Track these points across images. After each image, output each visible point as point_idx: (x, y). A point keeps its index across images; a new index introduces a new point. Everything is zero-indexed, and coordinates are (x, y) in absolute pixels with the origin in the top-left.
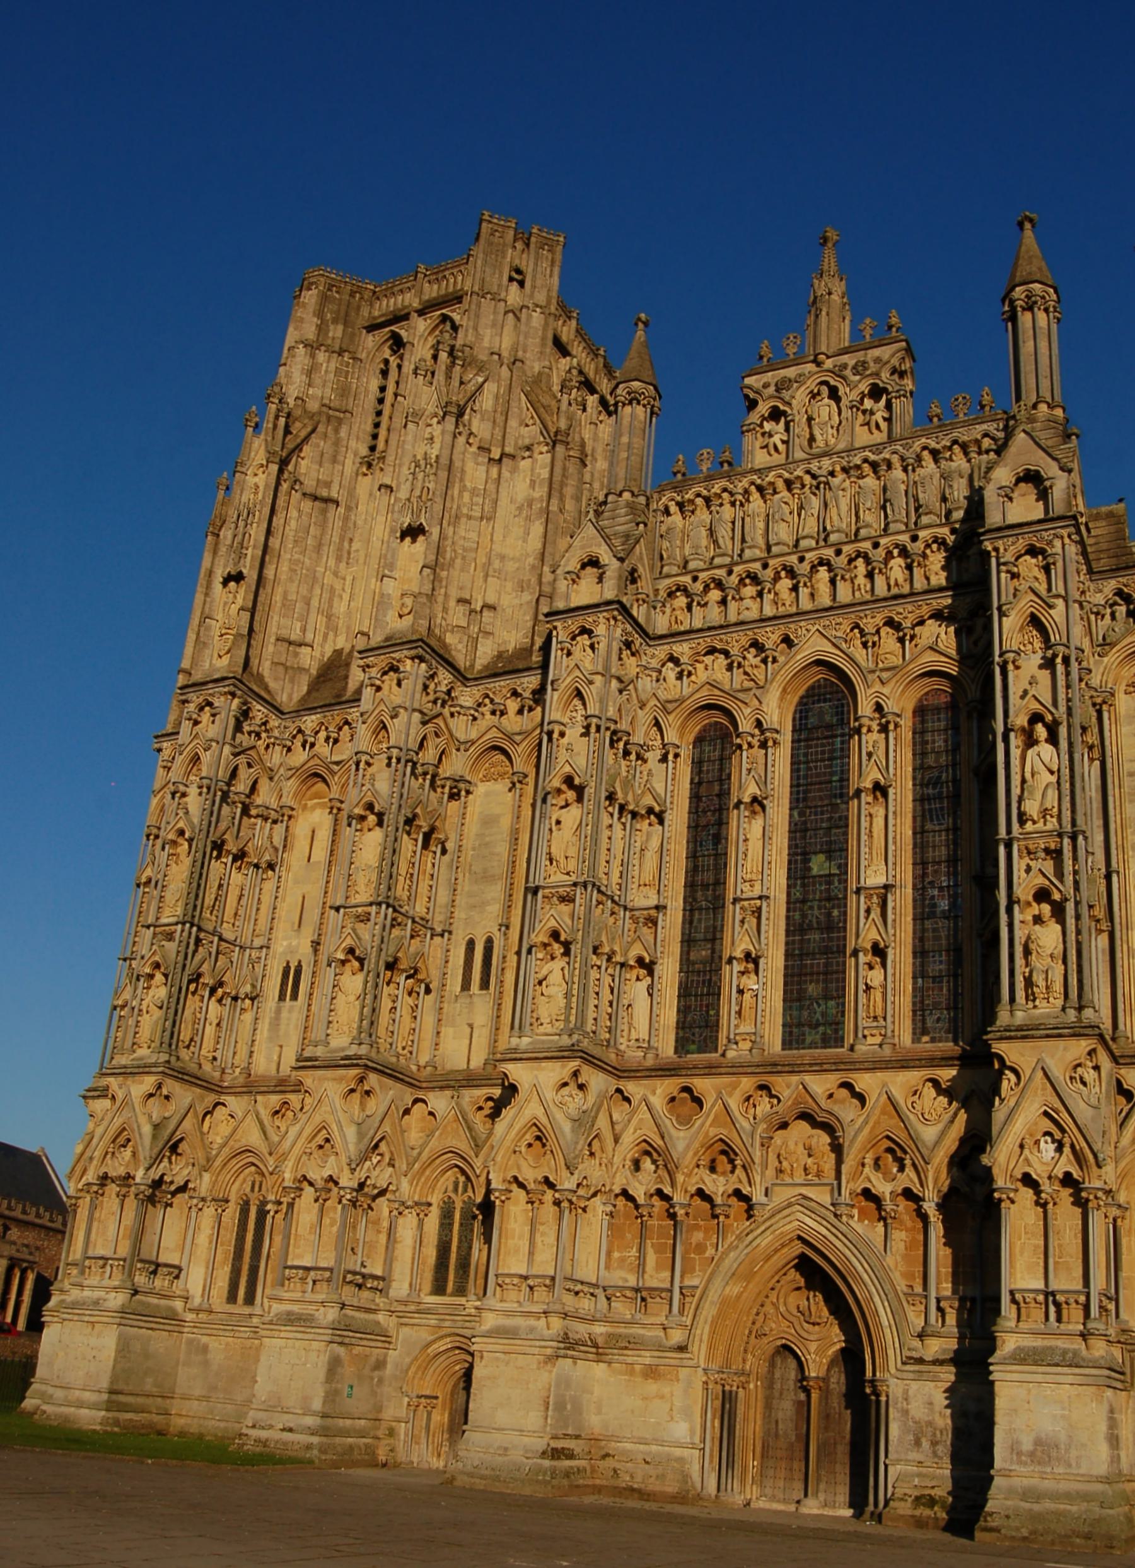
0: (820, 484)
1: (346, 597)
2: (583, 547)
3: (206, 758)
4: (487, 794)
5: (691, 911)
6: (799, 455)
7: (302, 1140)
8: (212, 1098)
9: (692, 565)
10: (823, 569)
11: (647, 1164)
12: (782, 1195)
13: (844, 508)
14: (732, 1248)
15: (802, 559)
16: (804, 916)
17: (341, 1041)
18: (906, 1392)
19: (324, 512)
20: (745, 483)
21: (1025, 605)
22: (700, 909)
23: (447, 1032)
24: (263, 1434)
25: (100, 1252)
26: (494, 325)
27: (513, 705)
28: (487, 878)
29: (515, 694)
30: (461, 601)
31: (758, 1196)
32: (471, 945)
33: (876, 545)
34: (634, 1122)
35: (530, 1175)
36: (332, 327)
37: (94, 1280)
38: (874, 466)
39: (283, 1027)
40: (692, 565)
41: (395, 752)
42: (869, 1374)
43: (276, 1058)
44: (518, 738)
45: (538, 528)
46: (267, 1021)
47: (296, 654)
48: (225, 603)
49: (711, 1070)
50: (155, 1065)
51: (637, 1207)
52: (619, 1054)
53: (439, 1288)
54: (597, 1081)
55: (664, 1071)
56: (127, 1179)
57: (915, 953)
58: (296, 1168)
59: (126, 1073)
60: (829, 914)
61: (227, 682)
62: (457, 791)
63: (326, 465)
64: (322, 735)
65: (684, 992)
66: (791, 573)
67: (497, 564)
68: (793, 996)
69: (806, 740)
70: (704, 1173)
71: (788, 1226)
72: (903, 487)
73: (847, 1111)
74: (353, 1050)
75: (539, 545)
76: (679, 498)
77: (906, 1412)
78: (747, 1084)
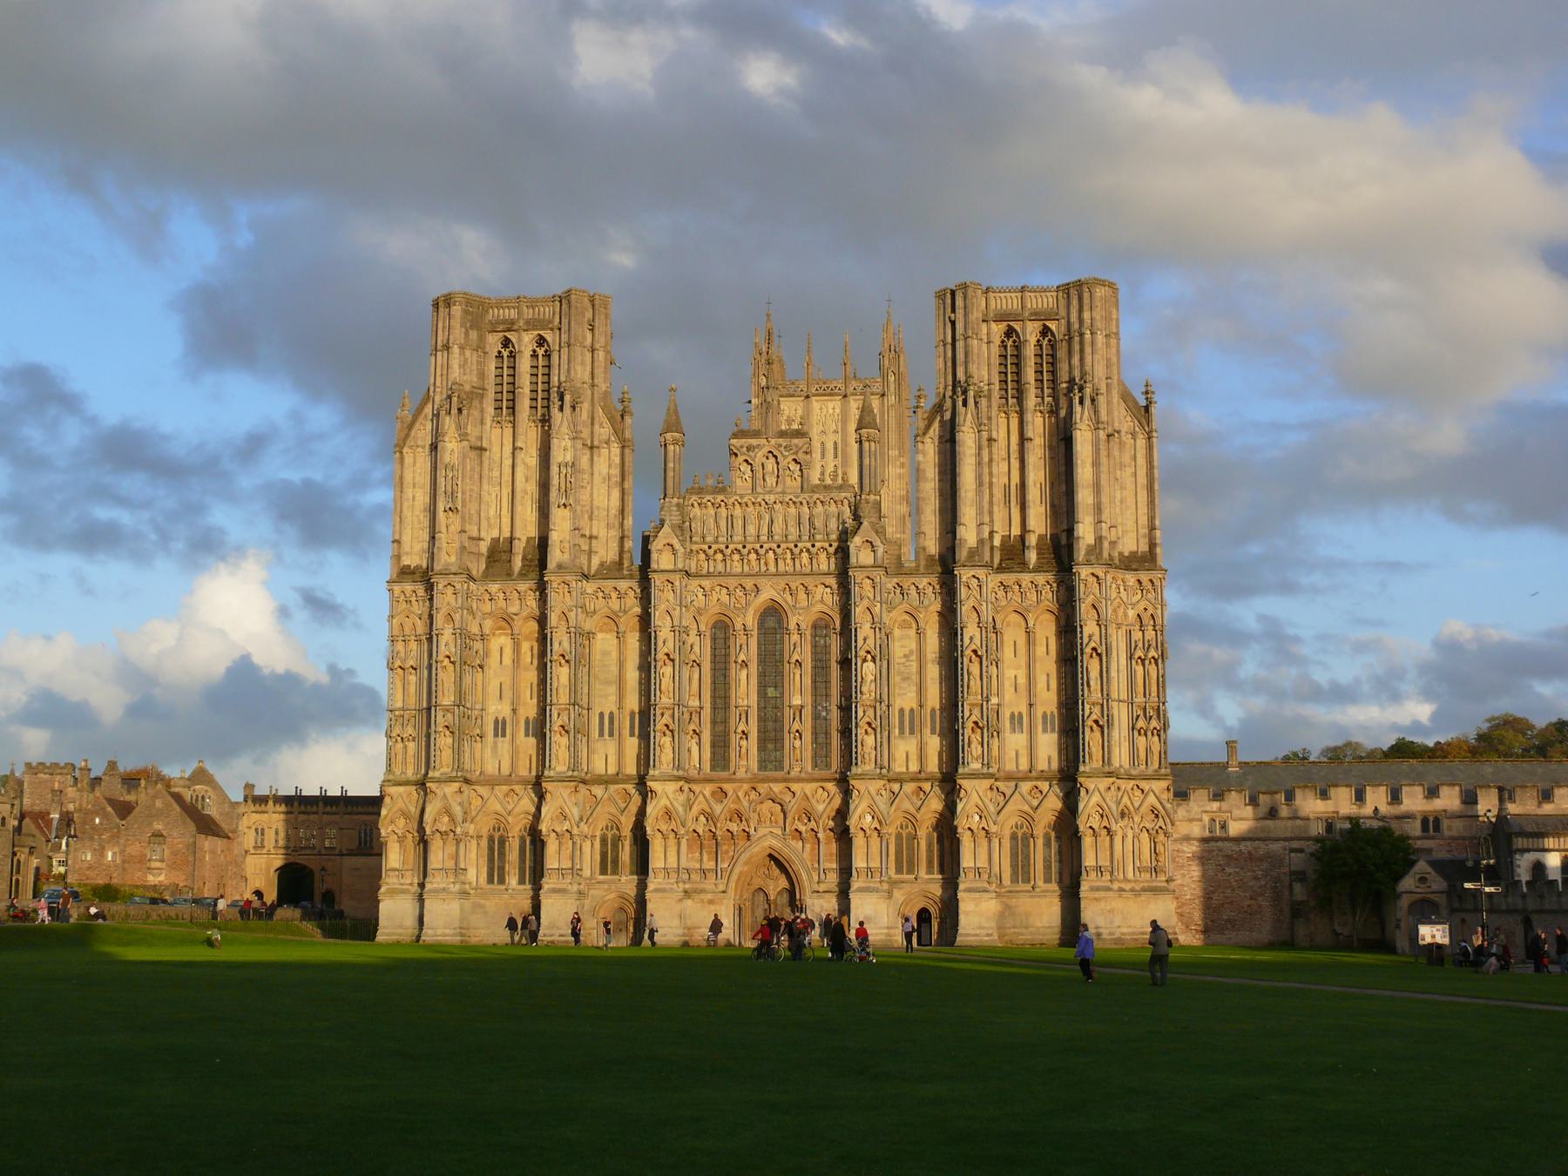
0: (770, 509)
4: (603, 639)
5: (715, 708)
10: (771, 552)
11: (702, 819)
13: (781, 522)
15: (761, 547)
16: (765, 714)
18: (813, 903)
19: (481, 456)
20: (732, 500)
21: (865, 603)
22: (718, 708)
24: (549, 939)
27: (614, 595)
28: (608, 683)
31: (752, 832)
33: (796, 546)
34: (697, 802)
35: (664, 828)
36: (471, 332)
37: (438, 879)
38: (794, 503)
39: (500, 752)
40: (709, 539)
41: (573, 630)
42: (798, 897)
43: (497, 766)
44: (621, 614)
45: (616, 493)
46: (489, 747)
47: (478, 546)
49: (729, 780)
51: (699, 837)
53: (603, 871)
54: (686, 788)
55: (708, 780)
57: (812, 734)
59: (439, 781)
60: (776, 715)
61: (463, 576)
65: (713, 745)
66: (756, 552)
67: (596, 513)
68: (762, 747)
70: (728, 822)
71: (766, 844)
72: (808, 517)
73: (787, 797)
74: (570, 773)
76: (699, 501)
77: (813, 911)
78: (746, 786)
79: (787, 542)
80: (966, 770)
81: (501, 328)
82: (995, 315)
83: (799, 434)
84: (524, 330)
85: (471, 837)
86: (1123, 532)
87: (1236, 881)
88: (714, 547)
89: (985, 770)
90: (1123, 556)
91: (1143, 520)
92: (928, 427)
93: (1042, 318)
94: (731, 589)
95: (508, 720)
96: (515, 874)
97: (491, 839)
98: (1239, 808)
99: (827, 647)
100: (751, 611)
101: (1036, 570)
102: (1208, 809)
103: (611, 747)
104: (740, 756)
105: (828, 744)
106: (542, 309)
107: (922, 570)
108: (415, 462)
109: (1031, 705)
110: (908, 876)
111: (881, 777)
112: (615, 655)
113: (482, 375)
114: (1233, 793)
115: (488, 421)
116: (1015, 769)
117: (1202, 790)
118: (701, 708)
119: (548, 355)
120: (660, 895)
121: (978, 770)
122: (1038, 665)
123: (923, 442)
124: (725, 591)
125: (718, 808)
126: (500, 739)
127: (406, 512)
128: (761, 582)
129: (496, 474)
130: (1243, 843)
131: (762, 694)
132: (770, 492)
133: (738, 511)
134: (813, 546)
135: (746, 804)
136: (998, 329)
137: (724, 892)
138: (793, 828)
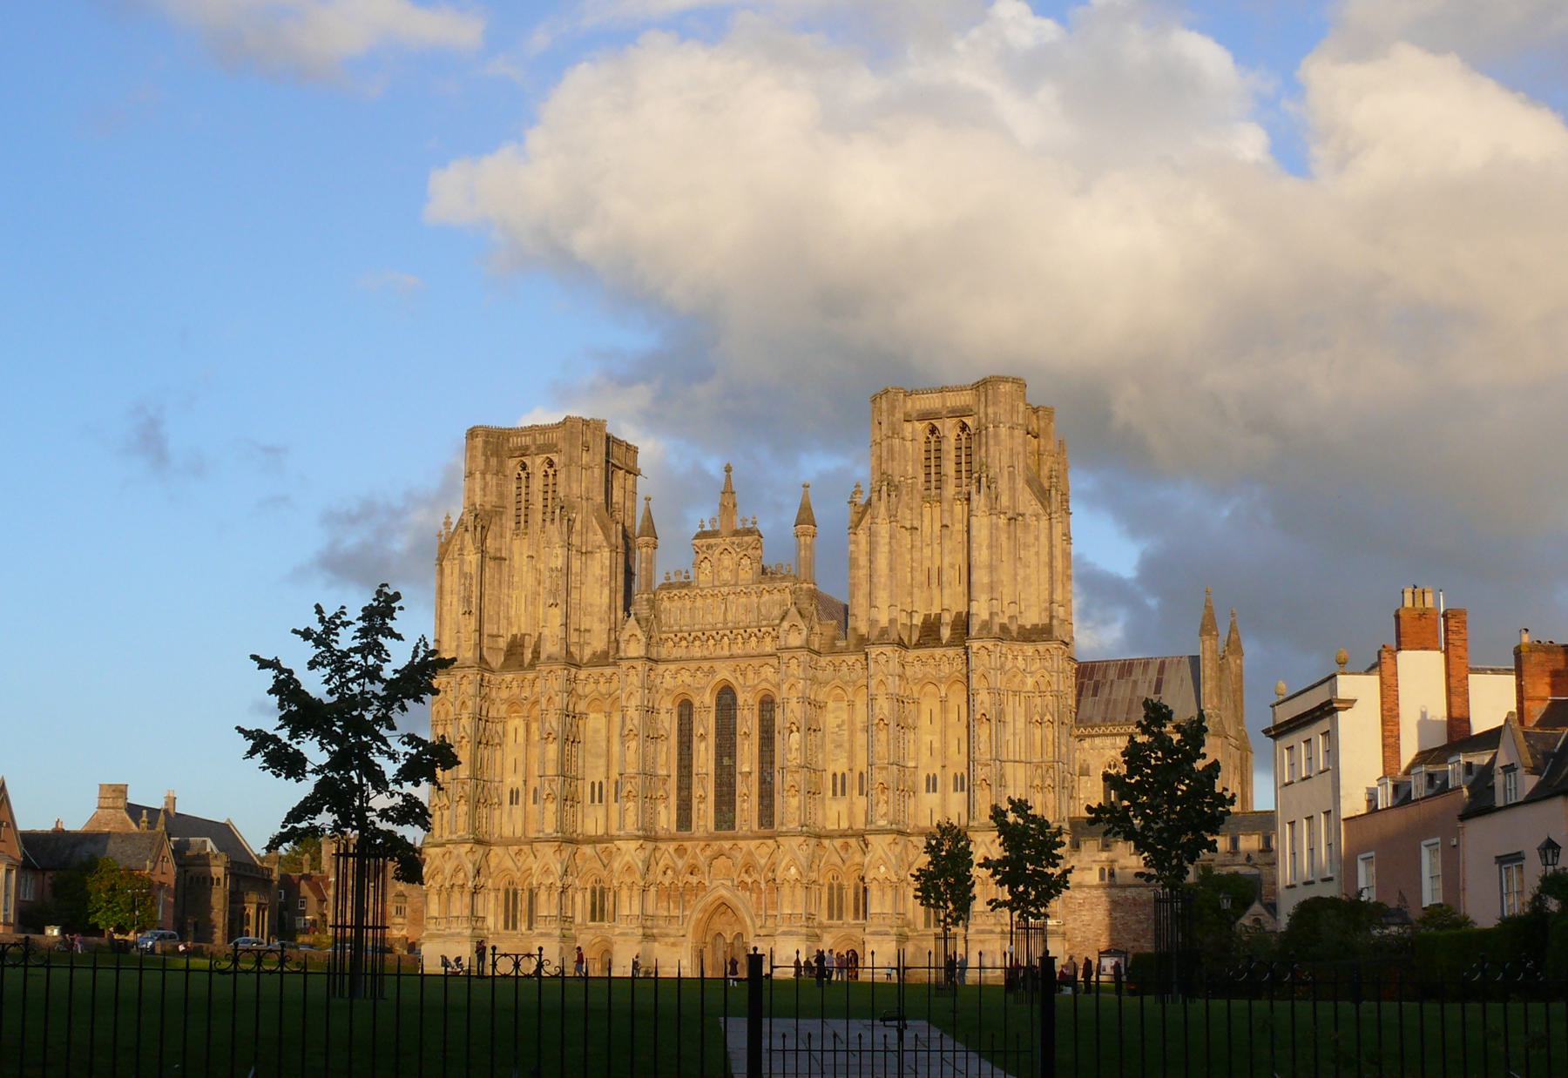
1: (514, 606)
2: (630, 630)
3: (470, 703)
6: (716, 583)
7: (539, 869)
8: (488, 849)
9: (676, 628)
10: (726, 638)
12: (714, 885)
14: (700, 901)
17: (549, 829)
19: (500, 565)
20: (694, 593)
21: (792, 680)
23: (587, 820)
25: (455, 914)
26: (577, 481)
27: (602, 680)
30: (576, 630)
31: (707, 884)
32: (593, 783)
34: (663, 858)
36: (491, 459)
45: (606, 591)
47: (497, 642)
48: (466, 626)
49: (690, 839)
50: (468, 839)
52: (656, 832)
53: (593, 919)
55: (673, 839)
56: (462, 886)
58: (537, 880)
62: (583, 715)
63: (498, 539)
64: (515, 683)
65: (679, 808)
66: (713, 638)
67: (589, 609)
72: (756, 605)
74: (555, 835)
75: (608, 600)
78: (702, 844)
79: (737, 628)
80: (873, 827)
81: (517, 453)
82: (918, 415)
83: (749, 532)
84: (536, 455)
85: (490, 890)
86: (1025, 606)
87: (1121, 924)
88: (679, 635)
89: (889, 827)
90: (1026, 629)
91: (1045, 596)
92: (860, 520)
93: (958, 415)
96: (525, 921)
98: (1125, 857)
100: (708, 691)
101: (948, 645)
102: (1097, 858)
103: (600, 811)
104: (698, 818)
106: (550, 435)
107: (852, 648)
108: (452, 573)
109: (944, 767)
110: (838, 922)
111: (801, 834)
112: (604, 732)
113: (501, 495)
114: (1120, 843)
115: (508, 535)
116: (929, 825)
117: (1092, 842)
118: (669, 776)
119: (555, 475)
120: (623, 938)
121: (882, 826)
122: (950, 732)
123: (855, 534)
125: (680, 863)
126: (514, 806)
127: (444, 614)
128: (717, 665)
130: (1129, 890)
132: (725, 585)
134: (760, 631)
136: (921, 427)
137: (683, 936)
138: (740, 880)
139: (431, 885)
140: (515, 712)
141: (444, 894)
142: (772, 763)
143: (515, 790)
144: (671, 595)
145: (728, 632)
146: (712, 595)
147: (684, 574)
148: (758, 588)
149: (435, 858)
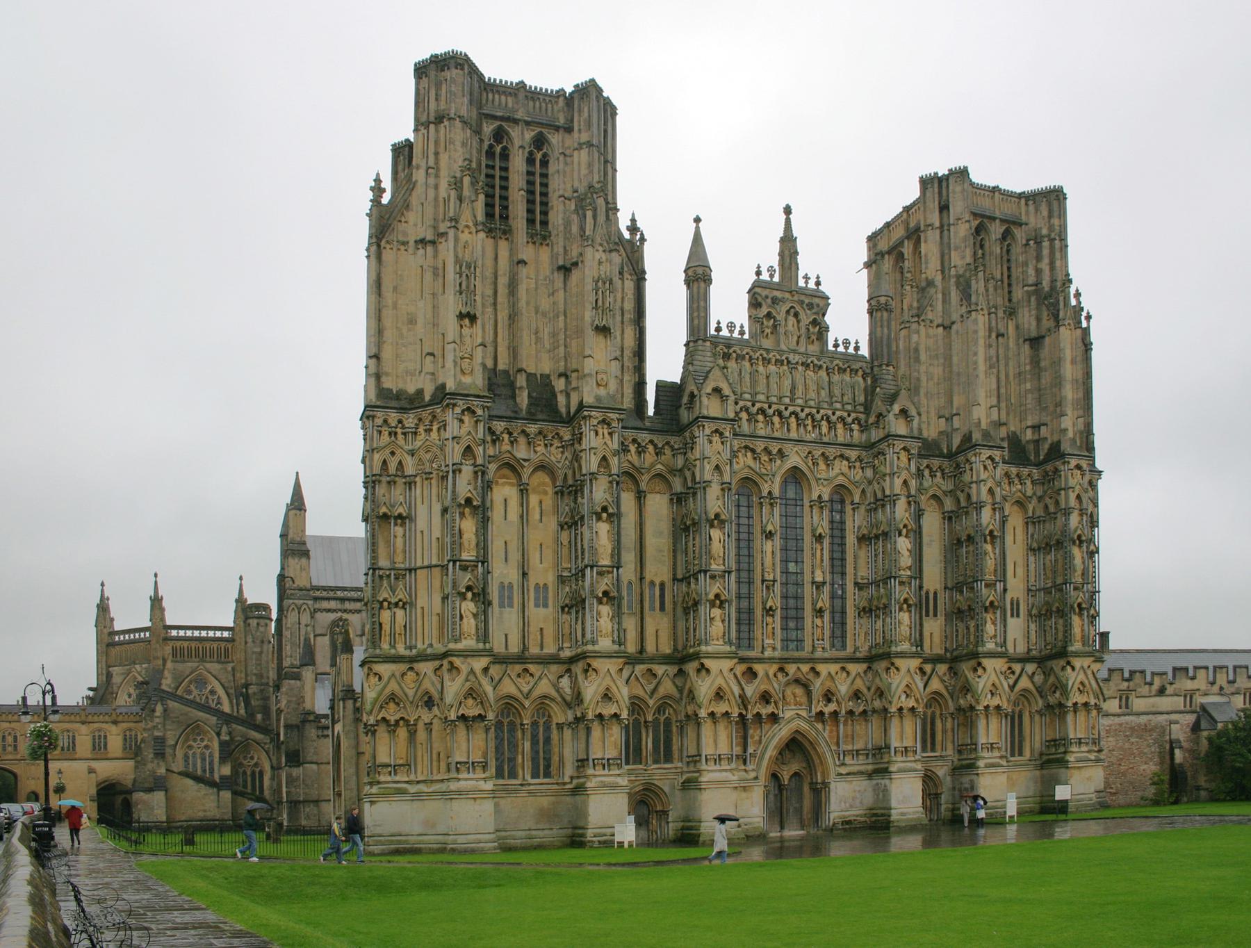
6: (783, 347)
20: (758, 354)
27: (633, 448)
29: (634, 441)
33: (818, 412)
44: (643, 471)
45: (630, 333)
65: (739, 623)
66: (780, 414)
68: (785, 628)
69: (786, 505)
79: (811, 407)
94: (758, 451)
95: (515, 587)
97: (499, 725)
99: (842, 522)
100: (778, 480)
105: (843, 624)
124: (749, 454)
126: (508, 609)
128: (788, 448)
129: (490, 292)
130: (1142, 717)
131: (785, 572)
132: (794, 351)
133: (761, 369)
134: (834, 414)
135: (776, 685)
139: (384, 719)
140: (504, 477)
141: (402, 732)
142: (843, 574)
143: (506, 584)
144: (731, 351)
145: (799, 409)
146: (777, 360)
147: (738, 329)
148: (832, 362)
149: (390, 679)
